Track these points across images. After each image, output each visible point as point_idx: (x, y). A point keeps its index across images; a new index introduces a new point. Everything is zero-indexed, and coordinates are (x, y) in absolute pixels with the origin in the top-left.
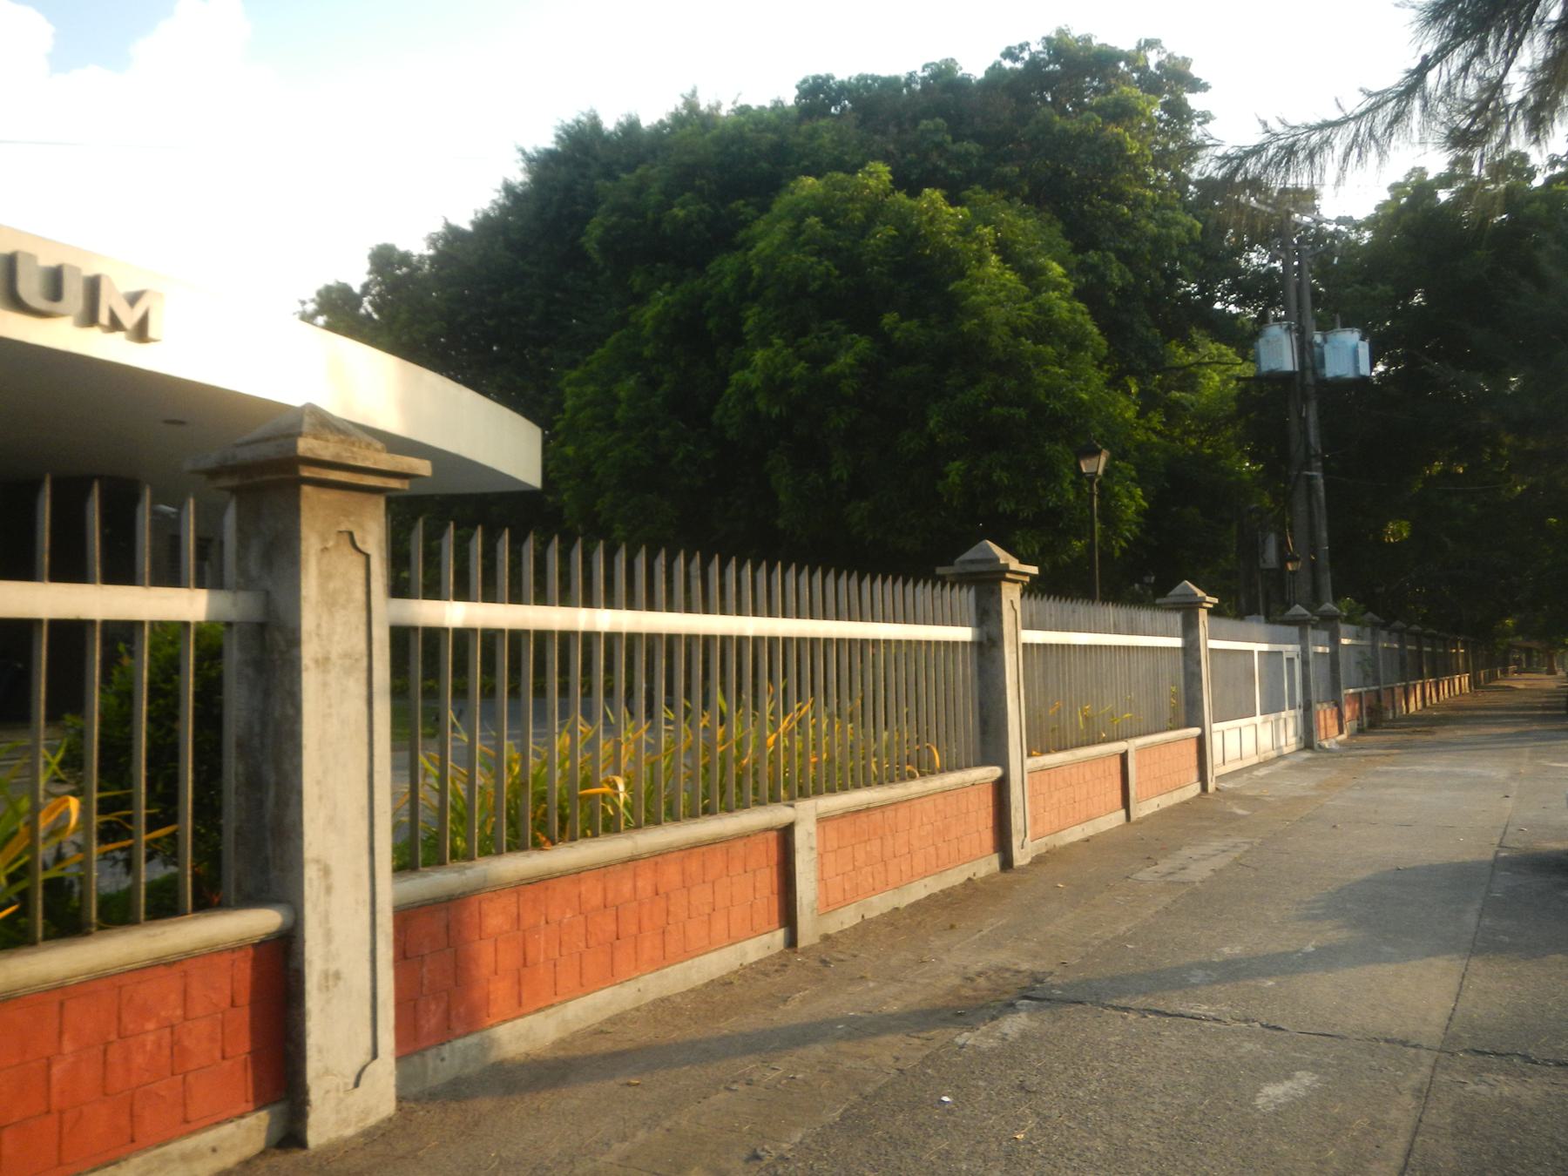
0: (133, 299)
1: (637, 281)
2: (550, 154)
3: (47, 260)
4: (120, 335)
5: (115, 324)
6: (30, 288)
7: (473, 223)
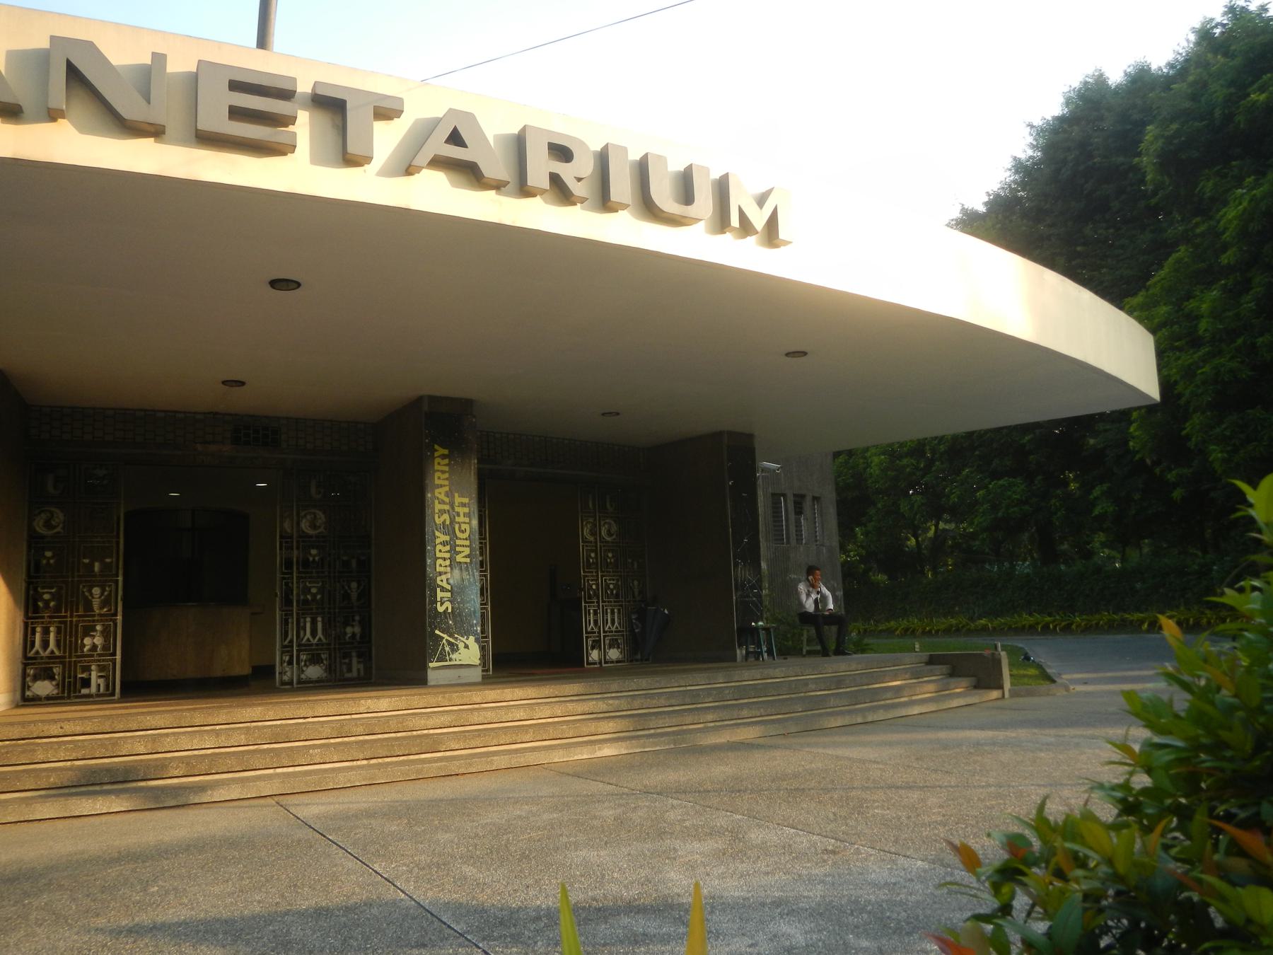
0: (761, 200)
1: (1208, 186)
2: (1061, 120)
3: (676, 165)
4: (752, 240)
5: (746, 227)
6: (663, 195)
7: (986, 204)
